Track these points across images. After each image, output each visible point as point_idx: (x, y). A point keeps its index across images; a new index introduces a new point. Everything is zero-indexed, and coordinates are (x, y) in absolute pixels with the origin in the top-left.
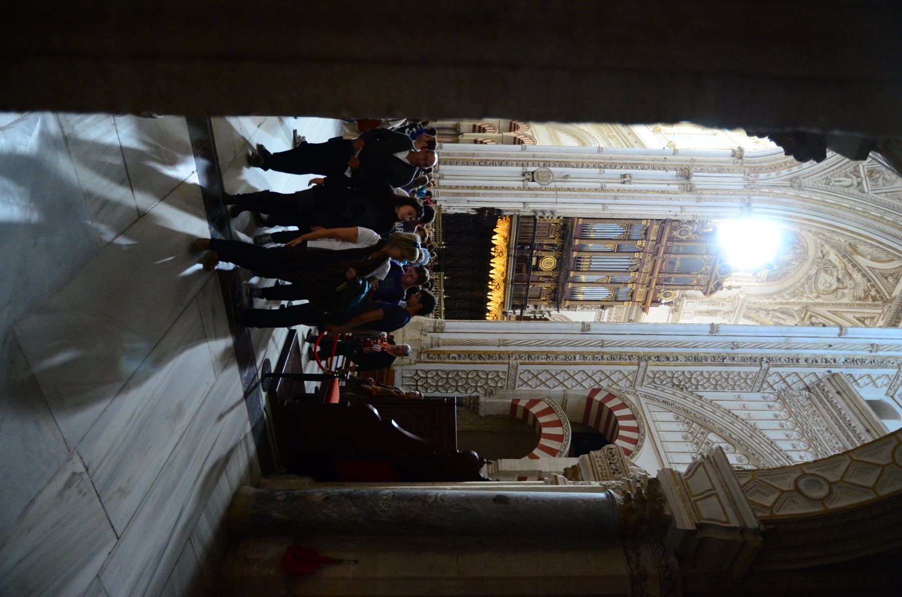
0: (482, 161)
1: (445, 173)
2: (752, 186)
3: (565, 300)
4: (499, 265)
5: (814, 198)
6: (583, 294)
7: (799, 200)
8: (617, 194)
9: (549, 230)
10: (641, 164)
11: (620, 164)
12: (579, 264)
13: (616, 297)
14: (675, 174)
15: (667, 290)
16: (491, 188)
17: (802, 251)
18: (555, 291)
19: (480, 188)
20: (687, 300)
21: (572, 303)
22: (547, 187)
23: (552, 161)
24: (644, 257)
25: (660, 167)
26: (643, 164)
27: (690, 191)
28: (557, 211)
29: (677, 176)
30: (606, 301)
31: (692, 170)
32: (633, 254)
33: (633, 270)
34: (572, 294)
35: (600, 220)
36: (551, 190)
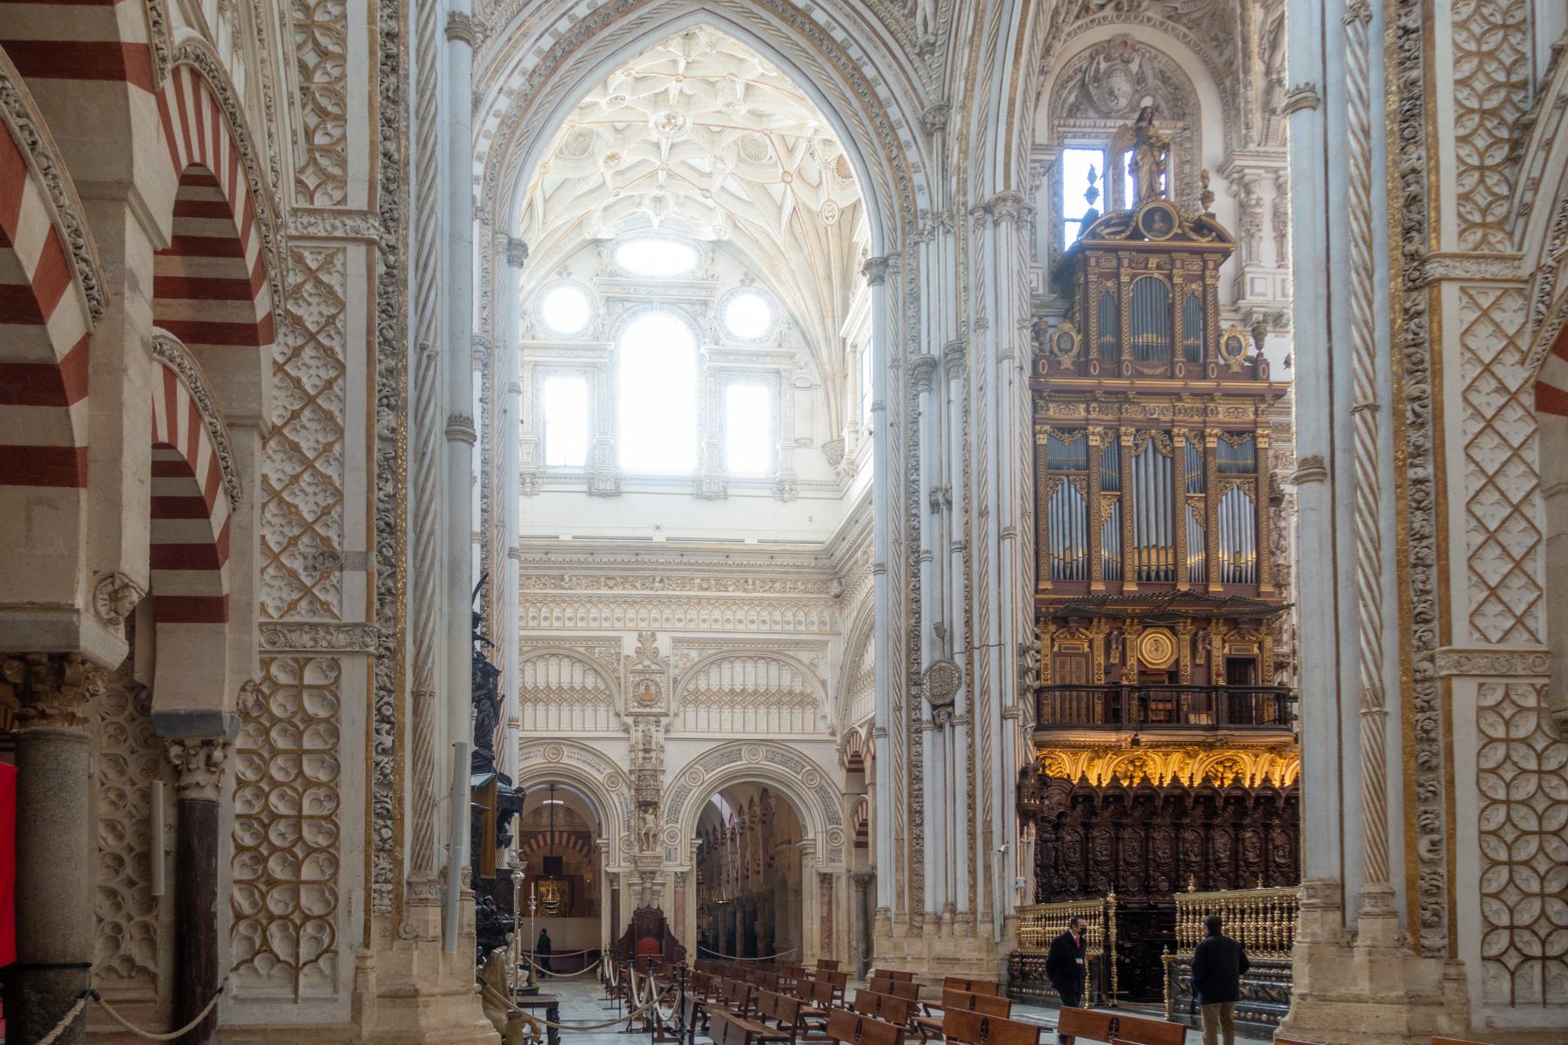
0: (911, 821)
1: (942, 899)
2: (945, 216)
3: (1258, 595)
4: (1166, 764)
5: (965, 66)
6: (1240, 552)
7: (972, 97)
8: (975, 514)
9: (1070, 655)
10: (906, 474)
11: (908, 521)
12: (1158, 573)
13: (1245, 471)
14: (926, 394)
15: (1219, 350)
16: (971, 795)
17: (1102, 57)
18: (1233, 623)
19: (972, 821)
20: (1248, 297)
21: (1265, 576)
22: (963, 672)
23: (908, 668)
24: (1131, 422)
25: (910, 433)
26: (907, 469)
27: (962, 351)
28: (1020, 641)
29: (930, 390)
30: (1257, 495)
31: (914, 358)
32: (1124, 451)
33: (1168, 442)
34: (1240, 581)
35: (1041, 541)
36: (970, 663)
